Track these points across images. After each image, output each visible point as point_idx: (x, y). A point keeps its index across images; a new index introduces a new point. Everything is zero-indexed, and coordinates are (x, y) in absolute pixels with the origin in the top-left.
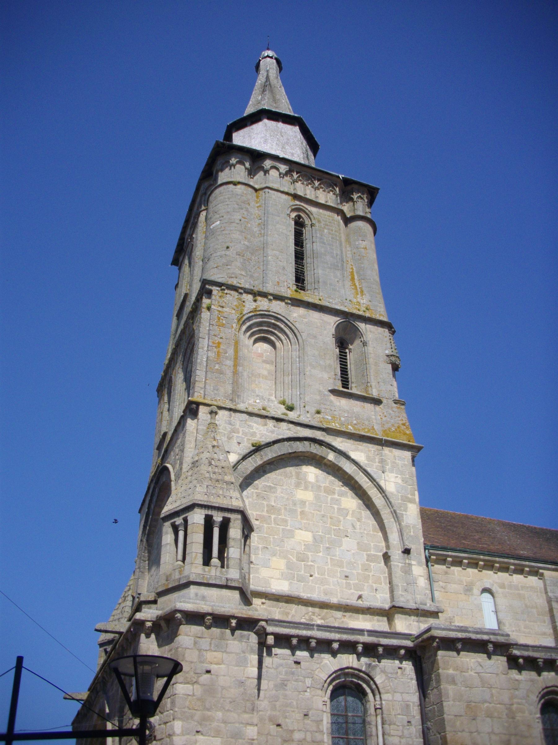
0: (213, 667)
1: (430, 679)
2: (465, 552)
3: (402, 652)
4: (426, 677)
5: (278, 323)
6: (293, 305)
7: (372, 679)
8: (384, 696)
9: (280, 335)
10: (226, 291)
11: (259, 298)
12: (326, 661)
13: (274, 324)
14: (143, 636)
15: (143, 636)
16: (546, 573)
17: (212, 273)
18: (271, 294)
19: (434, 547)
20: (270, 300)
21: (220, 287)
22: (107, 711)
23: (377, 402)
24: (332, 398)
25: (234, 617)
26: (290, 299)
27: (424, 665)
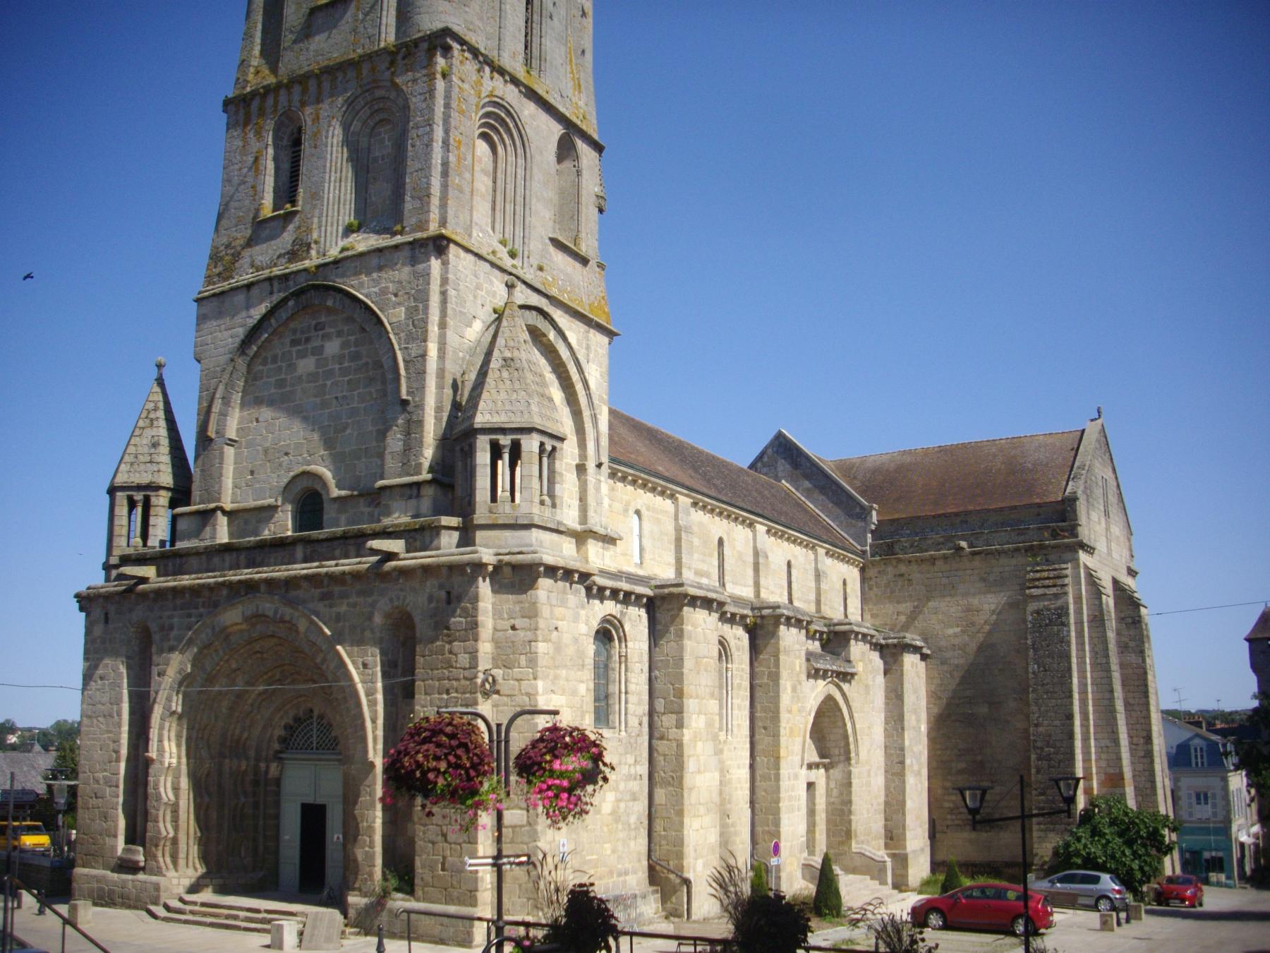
0: (560, 624)
1: (667, 631)
2: (631, 467)
3: (645, 600)
4: (659, 627)
5: (508, 120)
6: (526, 96)
7: (622, 626)
8: (630, 644)
9: (505, 136)
10: (466, 54)
11: (496, 75)
12: (597, 608)
13: (503, 120)
14: (480, 579)
15: (480, 579)
16: (681, 498)
17: (441, 9)
18: (510, 74)
19: (620, 463)
20: (506, 81)
21: (462, 45)
22: (328, 632)
23: (584, 261)
24: (552, 249)
25: (577, 571)
26: (526, 87)
27: (658, 615)
